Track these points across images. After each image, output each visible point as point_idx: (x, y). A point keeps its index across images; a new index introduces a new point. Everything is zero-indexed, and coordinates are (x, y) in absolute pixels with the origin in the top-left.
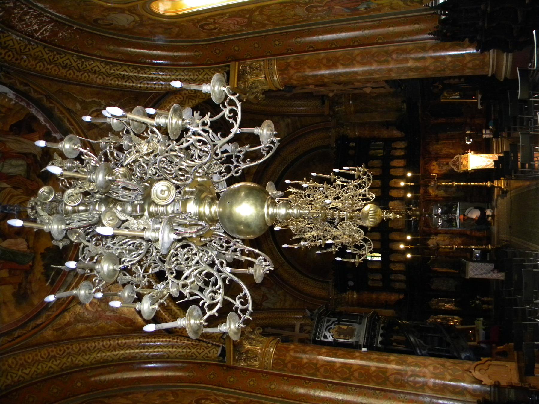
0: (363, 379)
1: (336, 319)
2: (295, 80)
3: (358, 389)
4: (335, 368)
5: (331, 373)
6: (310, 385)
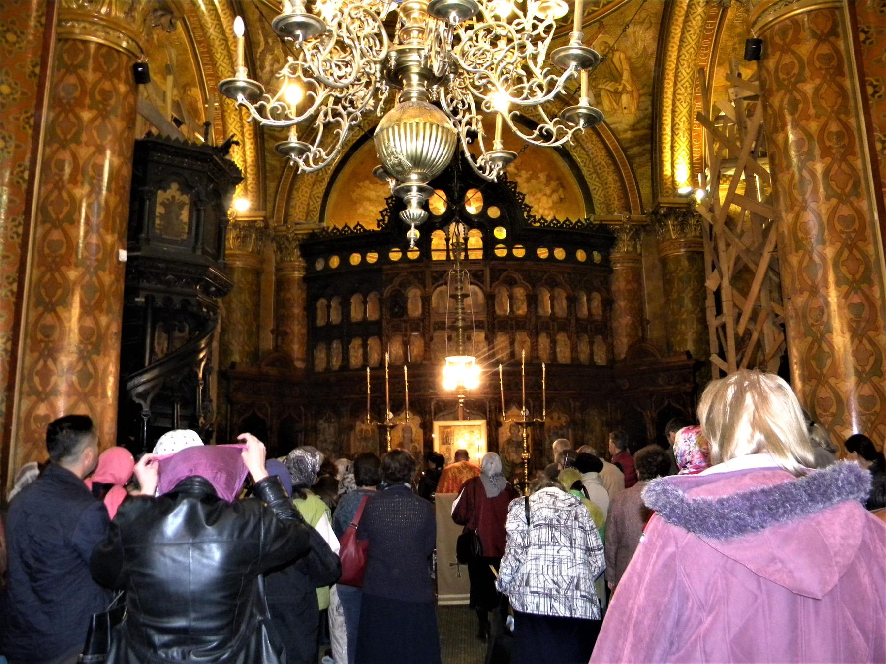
0: (46, 251)
2: (778, 63)
3: (18, 240)
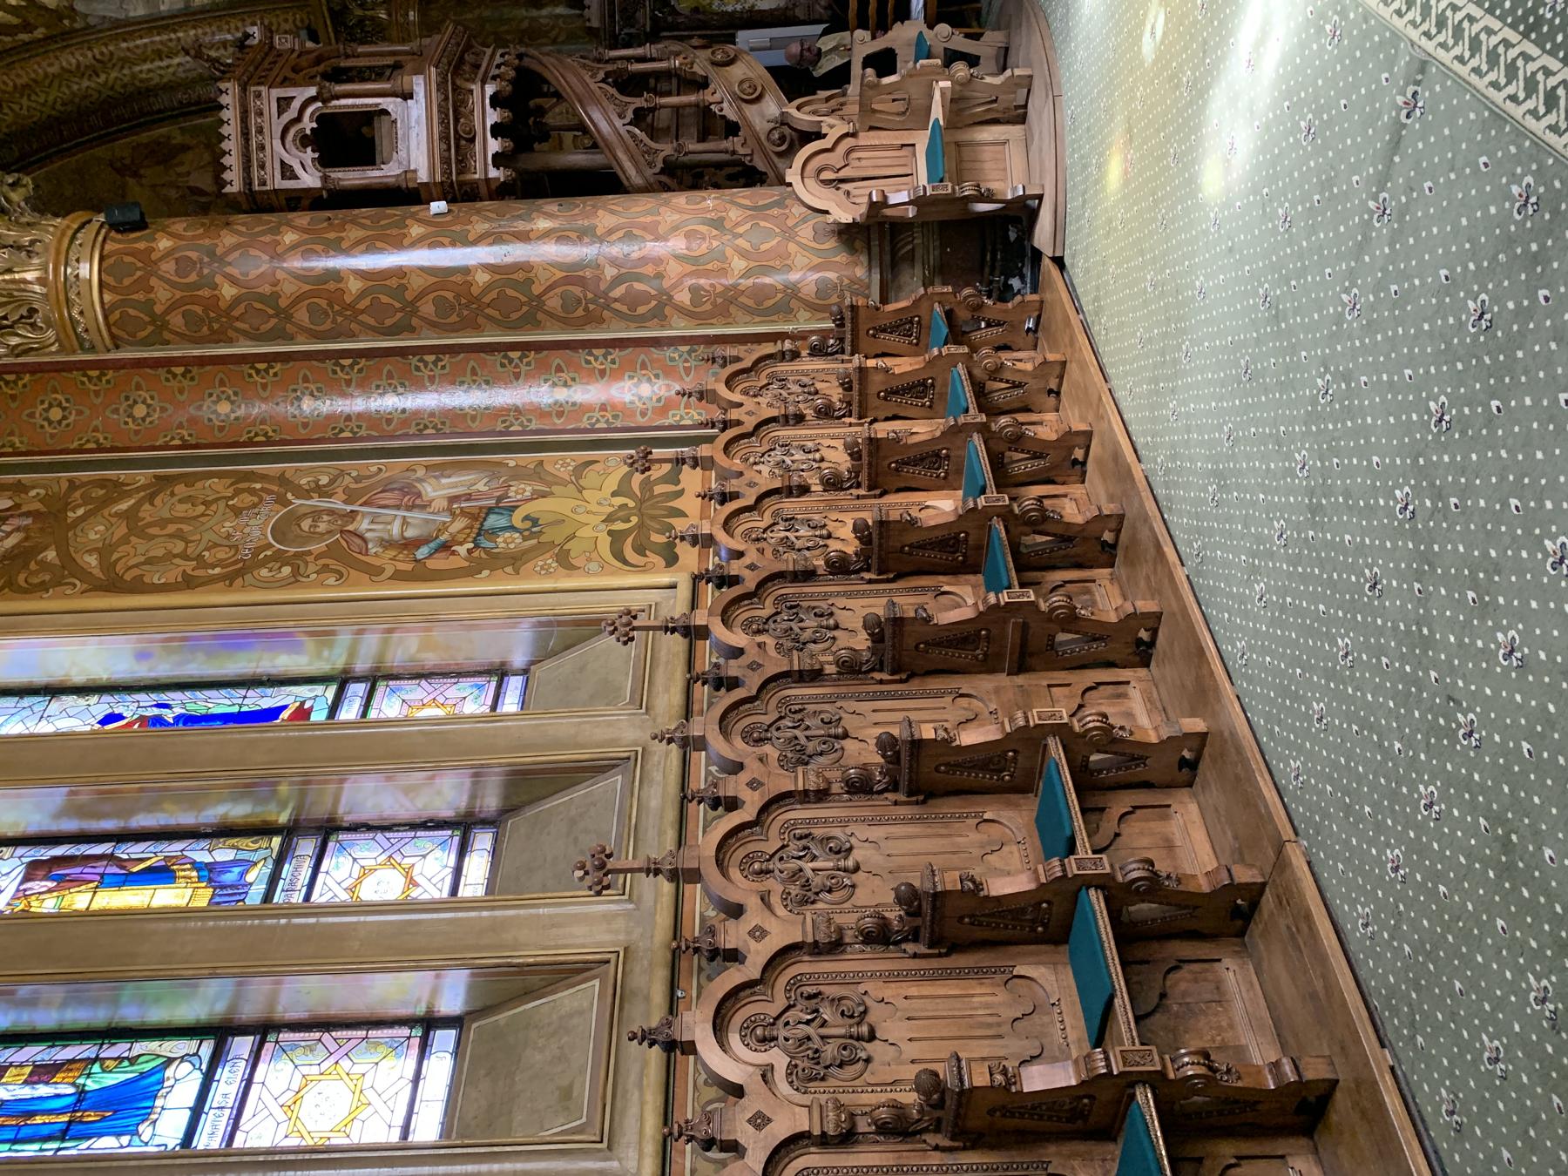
0: (454, 318)
1: (312, 91)
4: (348, 299)
5: (339, 319)
6: (275, 375)
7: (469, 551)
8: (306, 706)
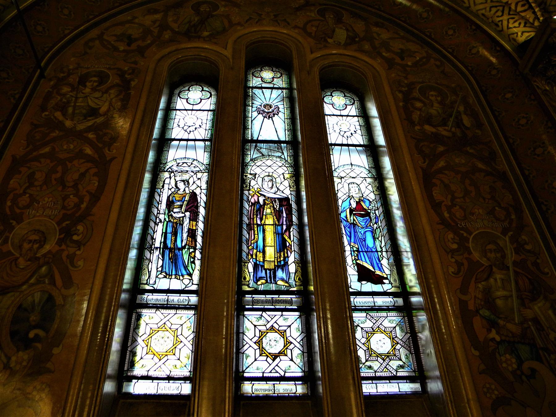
7: (493, 339)
8: (385, 281)
